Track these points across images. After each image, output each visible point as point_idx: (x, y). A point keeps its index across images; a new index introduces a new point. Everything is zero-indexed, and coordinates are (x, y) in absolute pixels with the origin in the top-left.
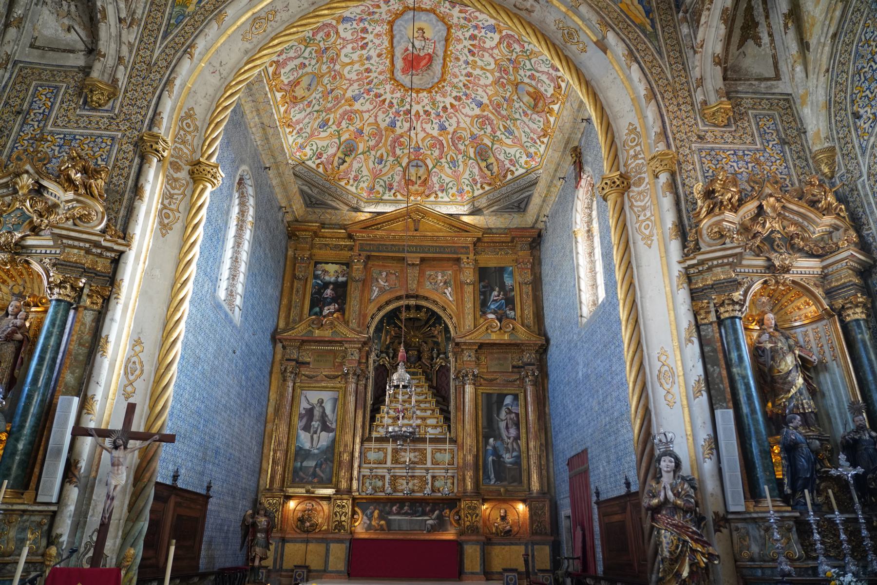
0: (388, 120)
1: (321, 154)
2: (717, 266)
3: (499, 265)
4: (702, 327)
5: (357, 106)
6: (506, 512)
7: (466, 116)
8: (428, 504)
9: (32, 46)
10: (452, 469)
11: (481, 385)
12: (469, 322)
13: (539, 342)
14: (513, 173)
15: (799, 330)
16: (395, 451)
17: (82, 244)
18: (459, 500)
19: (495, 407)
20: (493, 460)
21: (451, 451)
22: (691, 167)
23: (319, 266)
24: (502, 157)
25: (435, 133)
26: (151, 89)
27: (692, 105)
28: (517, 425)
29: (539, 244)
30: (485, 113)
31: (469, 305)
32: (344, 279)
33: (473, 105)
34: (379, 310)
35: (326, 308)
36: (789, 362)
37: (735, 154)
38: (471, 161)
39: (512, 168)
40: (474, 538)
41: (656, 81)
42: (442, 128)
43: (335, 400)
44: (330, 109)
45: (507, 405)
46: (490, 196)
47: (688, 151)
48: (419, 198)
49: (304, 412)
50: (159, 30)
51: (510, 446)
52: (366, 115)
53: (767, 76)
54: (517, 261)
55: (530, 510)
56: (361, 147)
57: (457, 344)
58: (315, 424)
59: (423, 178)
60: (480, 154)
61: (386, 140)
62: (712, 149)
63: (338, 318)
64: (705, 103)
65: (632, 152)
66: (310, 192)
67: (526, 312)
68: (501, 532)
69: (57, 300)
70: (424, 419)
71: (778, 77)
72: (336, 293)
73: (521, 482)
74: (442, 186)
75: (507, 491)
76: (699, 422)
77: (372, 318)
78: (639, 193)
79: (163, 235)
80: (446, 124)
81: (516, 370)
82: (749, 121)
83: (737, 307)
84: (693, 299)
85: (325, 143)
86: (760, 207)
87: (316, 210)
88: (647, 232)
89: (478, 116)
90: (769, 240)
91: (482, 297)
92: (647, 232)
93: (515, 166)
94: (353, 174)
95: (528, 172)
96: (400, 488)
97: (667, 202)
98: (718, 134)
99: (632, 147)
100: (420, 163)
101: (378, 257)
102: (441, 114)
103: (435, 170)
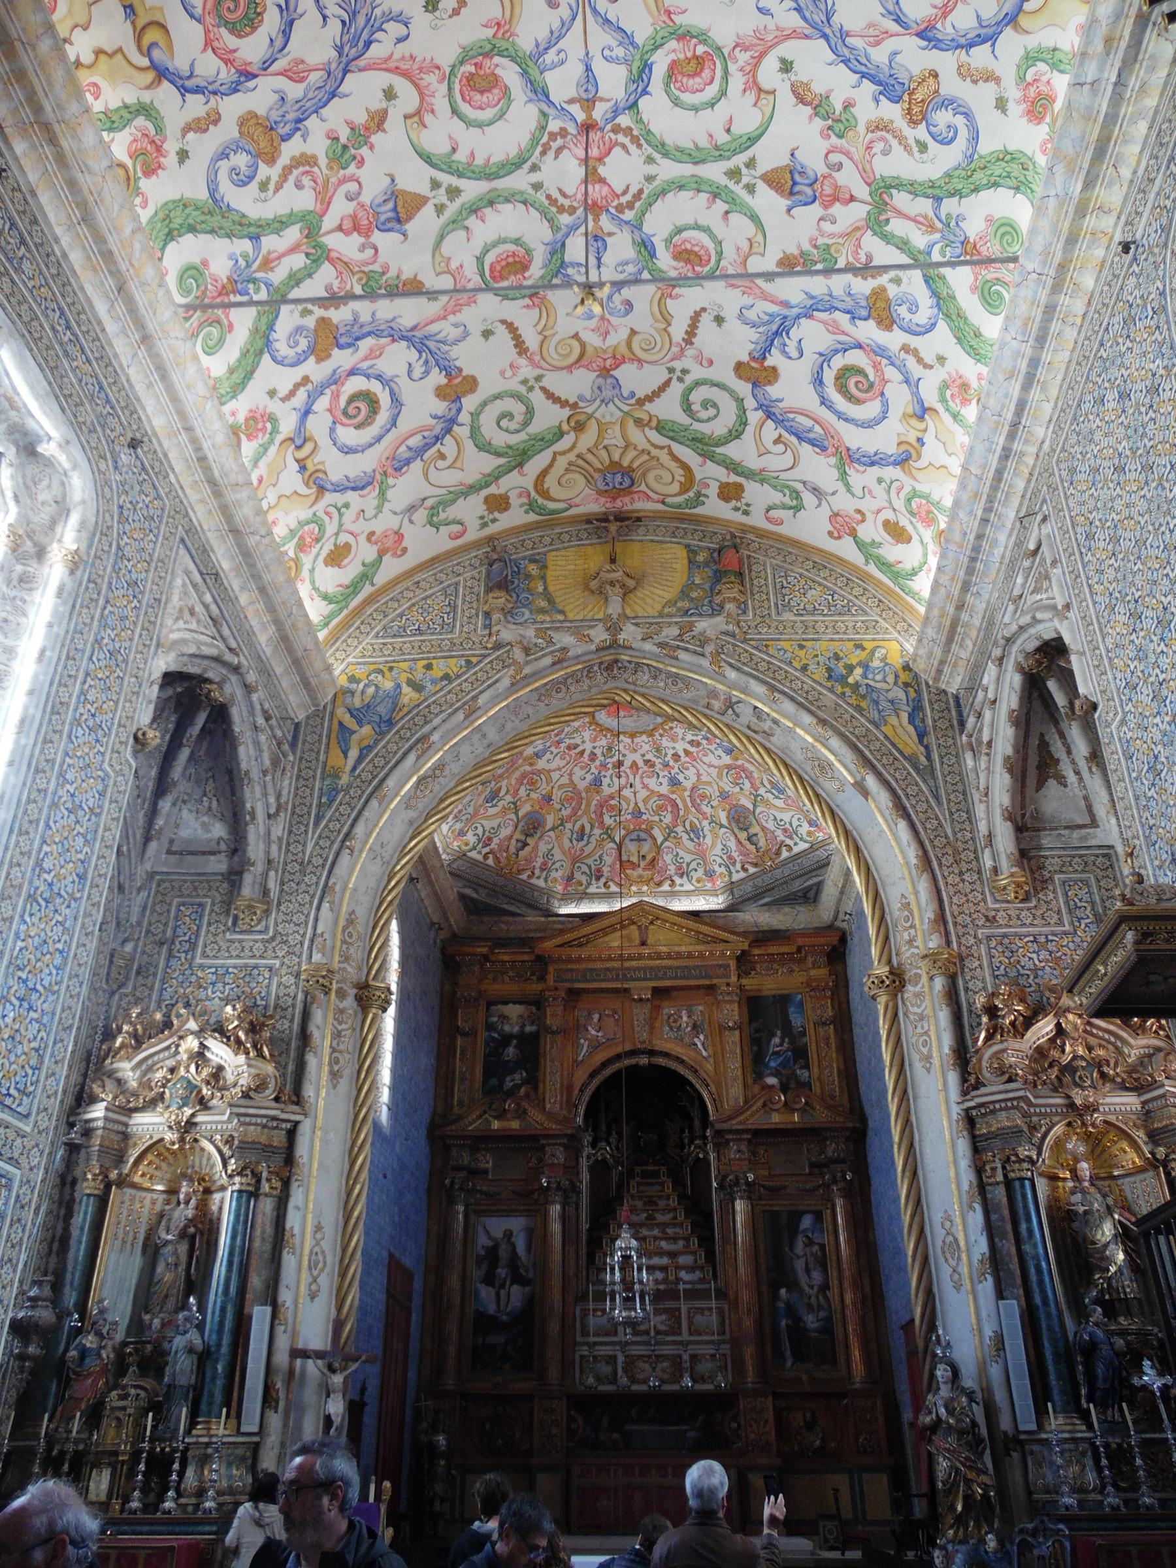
0: (589, 777)
1: (490, 839)
2: (1001, 1109)
4: (988, 1188)
5: (541, 764)
7: (710, 766)
9: (169, 852)
10: (723, 1342)
11: (760, 1199)
12: (734, 1093)
14: (790, 848)
15: (1127, 1180)
17: (259, 1120)
20: (788, 1326)
21: (720, 1312)
22: (977, 963)
23: (493, 1008)
24: (770, 825)
25: (664, 789)
26: (308, 898)
27: (979, 872)
28: (823, 1264)
29: (844, 954)
30: (740, 762)
31: (734, 1065)
32: (534, 1028)
33: (720, 752)
34: (592, 1076)
36: (1106, 1231)
37: (1035, 941)
38: (723, 830)
39: (788, 842)
41: (931, 841)
42: (674, 783)
43: (530, 1232)
44: (501, 776)
45: (805, 1230)
46: (759, 882)
47: (972, 941)
49: (482, 1253)
50: (309, 813)
52: (555, 776)
53: (1080, 822)
54: (808, 984)
56: (550, 820)
57: (719, 1133)
58: (502, 1272)
59: (649, 858)
60: (738, 822)
61: (588, 805)
62: (1005, 936)
63: (527, 1096)
64: (995, 870)
65: (906, 937)
66: (475, 895)
69: (240, 1192)
70: (672, 1255)
71: (1094, 823)
74: (680, 868)
76: (984, 1314)
77: (581, 1091)
78: (916, 995)
79: (335, 1087)
80: (681, 777)
81: (816, 1170)
82: (1054, 892)
83: (1025, 1165)
84: (976, 1150)
85: (495, 823)
86: (1058, 1025)
87: (485, 919)
88: (925, 1051)
89: (729, 767)
90: (1070, 1069)
92: (925, 1051)
93: (791, 838)
94: (540, 860)
95: (813, 848)
96: (641, 1376)
97: (944, 1016)
98: (1013, 913)
99: (906, 929)
100: (643, 835)
101: (587, 991)
102: (671, 763)
103: (667, 844)
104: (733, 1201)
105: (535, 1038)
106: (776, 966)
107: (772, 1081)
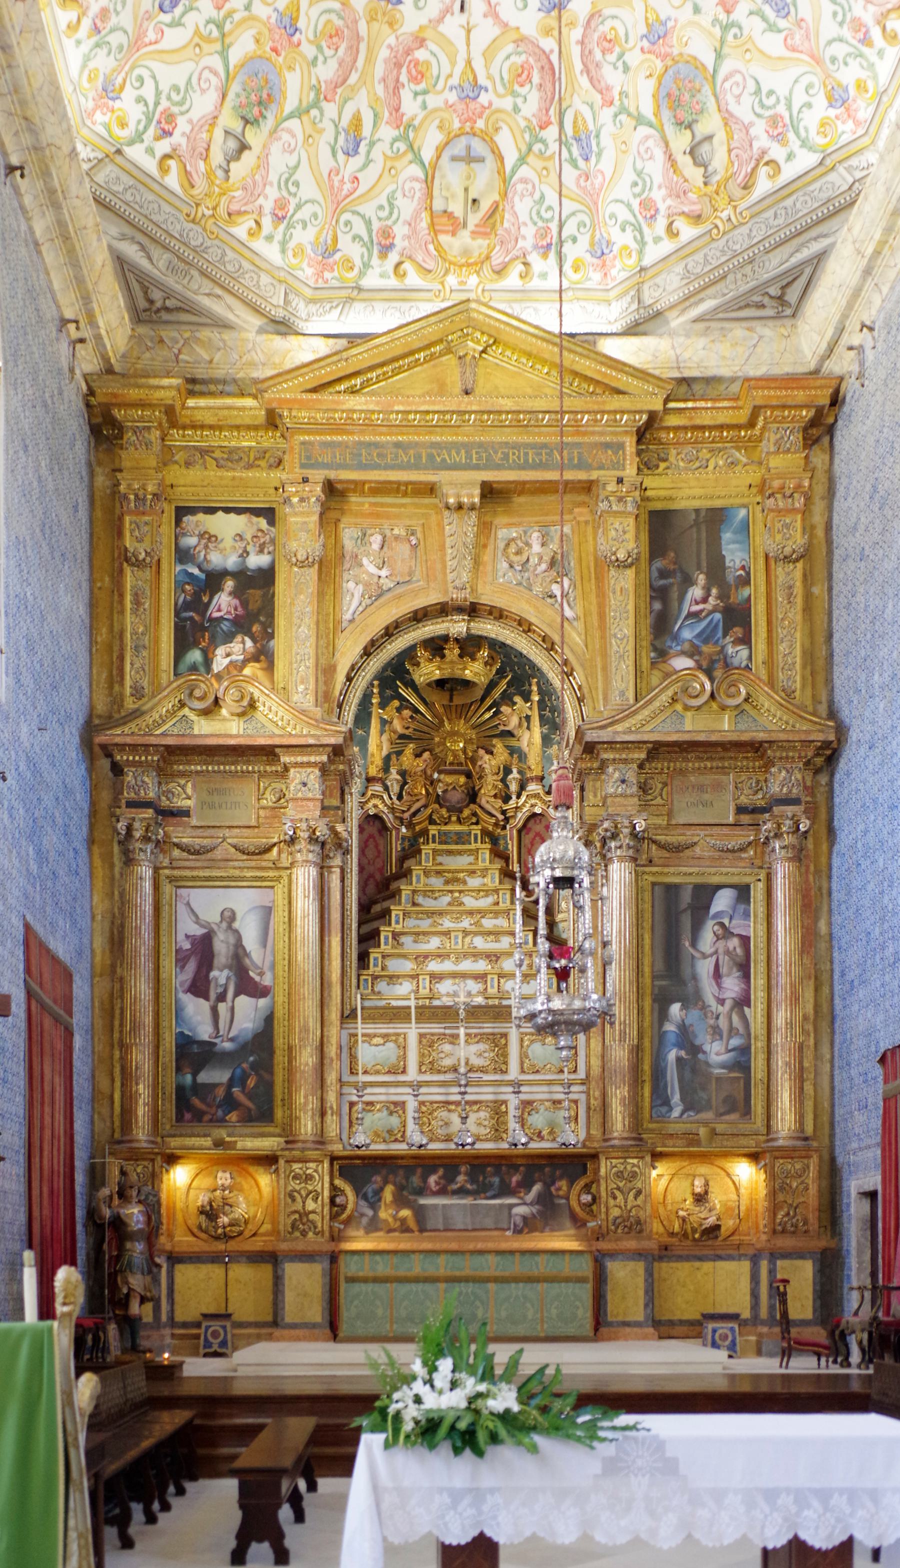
3: (710, 504)
6: (707, 1184)
8: (515, 1168)
13: (821, 737)
16: (427, 1042)
18: (594, 1157)
19: (686, 921)
23: (188, 520)
35: (220, 651)
40: (631, 1244)
43: (267, 912)
48: (473, 281)
51: (723, 1023)
54: (762, 487)
55: (772, 1177)
67: (783, 648)
68: (694, 1230)
72: (244, 604)
73: (747, 1112)
75: (713, 1133)
77: (349, 679)
81: (746, 819)
91: (657, 606)
104: (606, 861)
105: (267, 576)
106: (704, 454)
107: (682, 663)
